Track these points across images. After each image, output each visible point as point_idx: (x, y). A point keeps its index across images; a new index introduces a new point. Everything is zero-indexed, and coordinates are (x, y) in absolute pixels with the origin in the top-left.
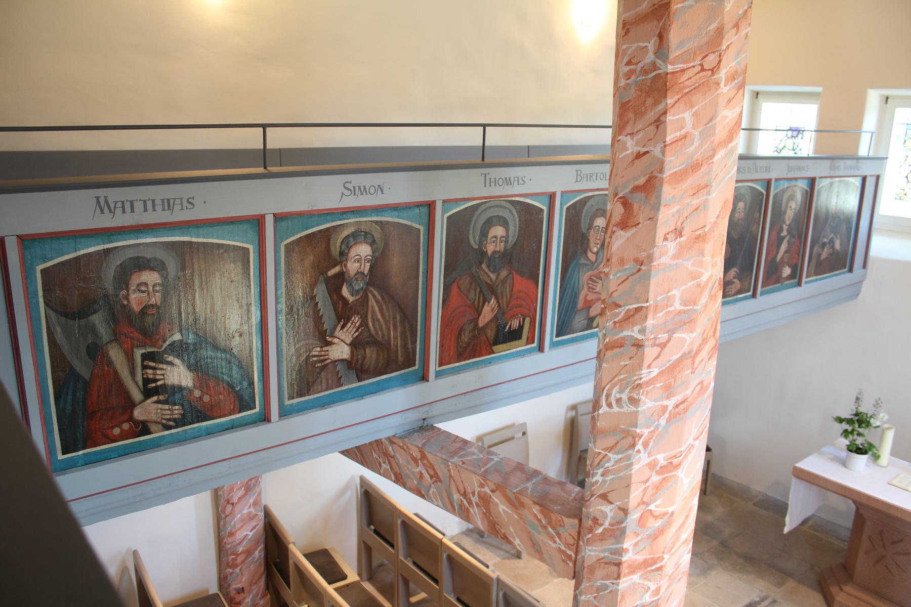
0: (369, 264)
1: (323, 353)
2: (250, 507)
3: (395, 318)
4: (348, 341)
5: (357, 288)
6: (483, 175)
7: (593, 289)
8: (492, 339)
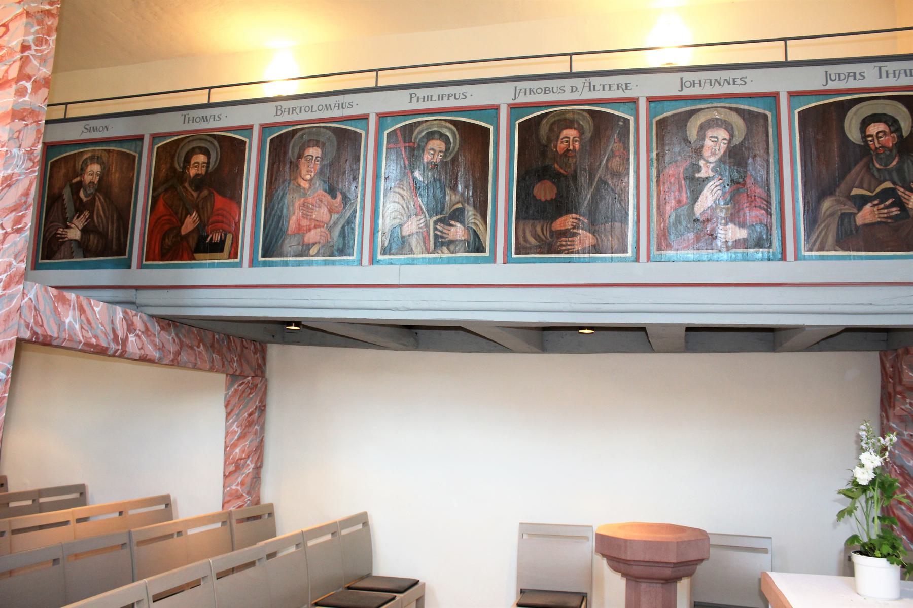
0: (98, 177)
1: (64, 233)
2: (237, 485)
4: (80, 228)
5: (89, 192)
6: (183, 116)
7: (307, 215)
8: (193, 246)
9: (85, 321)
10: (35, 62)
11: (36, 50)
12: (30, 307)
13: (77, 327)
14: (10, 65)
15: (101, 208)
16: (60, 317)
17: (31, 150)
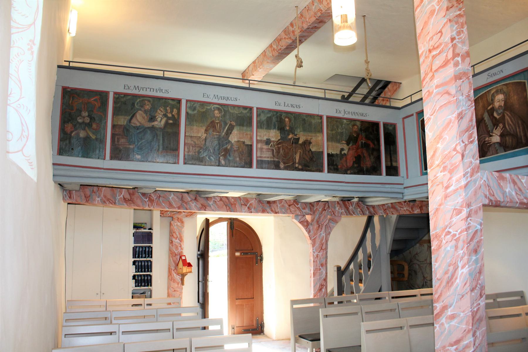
0: (503, 102)
1: (489, 140)
3: (518, 123)
4: (499, 134)
5: (500, 112)
9: (518, 190)
10: (459, 45)
11: (458, 39)
12: (485, 185)
13: (514, 193)
14: (448, 52)
15: (509, 120)
16: (503, 189)
17: (469, 94)
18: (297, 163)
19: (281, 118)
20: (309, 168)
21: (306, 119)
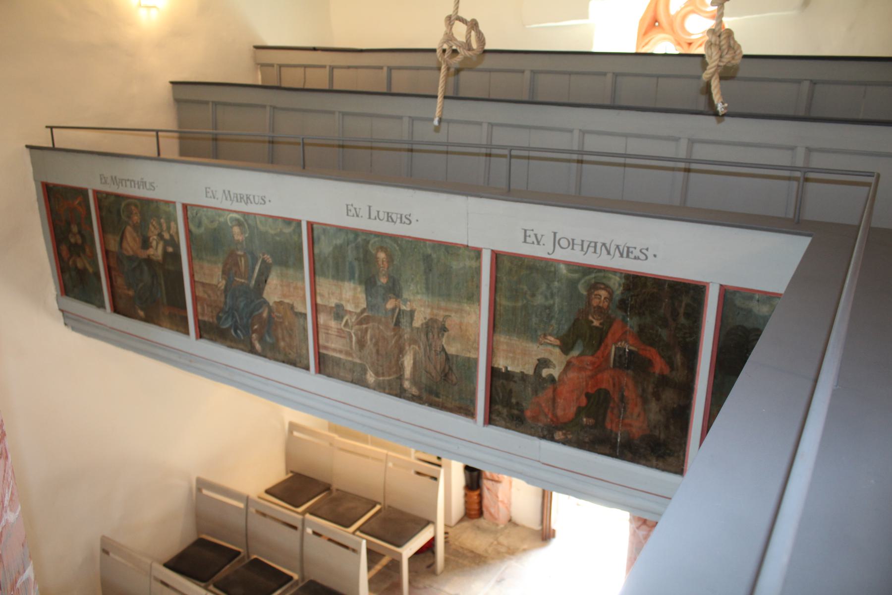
18: (407, 379)
19: (366, 252)
20: (437, 399)
21: (434, 256)
